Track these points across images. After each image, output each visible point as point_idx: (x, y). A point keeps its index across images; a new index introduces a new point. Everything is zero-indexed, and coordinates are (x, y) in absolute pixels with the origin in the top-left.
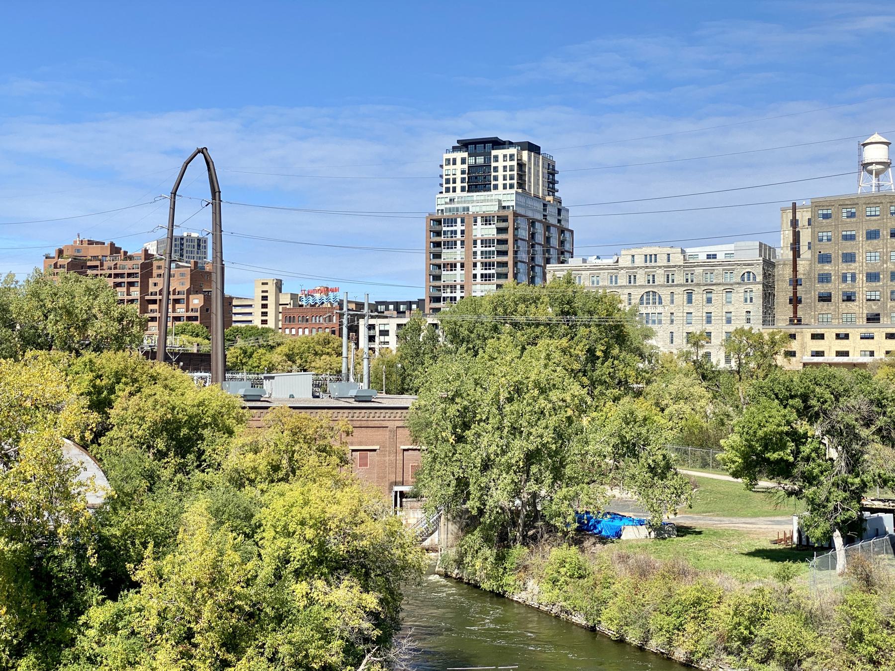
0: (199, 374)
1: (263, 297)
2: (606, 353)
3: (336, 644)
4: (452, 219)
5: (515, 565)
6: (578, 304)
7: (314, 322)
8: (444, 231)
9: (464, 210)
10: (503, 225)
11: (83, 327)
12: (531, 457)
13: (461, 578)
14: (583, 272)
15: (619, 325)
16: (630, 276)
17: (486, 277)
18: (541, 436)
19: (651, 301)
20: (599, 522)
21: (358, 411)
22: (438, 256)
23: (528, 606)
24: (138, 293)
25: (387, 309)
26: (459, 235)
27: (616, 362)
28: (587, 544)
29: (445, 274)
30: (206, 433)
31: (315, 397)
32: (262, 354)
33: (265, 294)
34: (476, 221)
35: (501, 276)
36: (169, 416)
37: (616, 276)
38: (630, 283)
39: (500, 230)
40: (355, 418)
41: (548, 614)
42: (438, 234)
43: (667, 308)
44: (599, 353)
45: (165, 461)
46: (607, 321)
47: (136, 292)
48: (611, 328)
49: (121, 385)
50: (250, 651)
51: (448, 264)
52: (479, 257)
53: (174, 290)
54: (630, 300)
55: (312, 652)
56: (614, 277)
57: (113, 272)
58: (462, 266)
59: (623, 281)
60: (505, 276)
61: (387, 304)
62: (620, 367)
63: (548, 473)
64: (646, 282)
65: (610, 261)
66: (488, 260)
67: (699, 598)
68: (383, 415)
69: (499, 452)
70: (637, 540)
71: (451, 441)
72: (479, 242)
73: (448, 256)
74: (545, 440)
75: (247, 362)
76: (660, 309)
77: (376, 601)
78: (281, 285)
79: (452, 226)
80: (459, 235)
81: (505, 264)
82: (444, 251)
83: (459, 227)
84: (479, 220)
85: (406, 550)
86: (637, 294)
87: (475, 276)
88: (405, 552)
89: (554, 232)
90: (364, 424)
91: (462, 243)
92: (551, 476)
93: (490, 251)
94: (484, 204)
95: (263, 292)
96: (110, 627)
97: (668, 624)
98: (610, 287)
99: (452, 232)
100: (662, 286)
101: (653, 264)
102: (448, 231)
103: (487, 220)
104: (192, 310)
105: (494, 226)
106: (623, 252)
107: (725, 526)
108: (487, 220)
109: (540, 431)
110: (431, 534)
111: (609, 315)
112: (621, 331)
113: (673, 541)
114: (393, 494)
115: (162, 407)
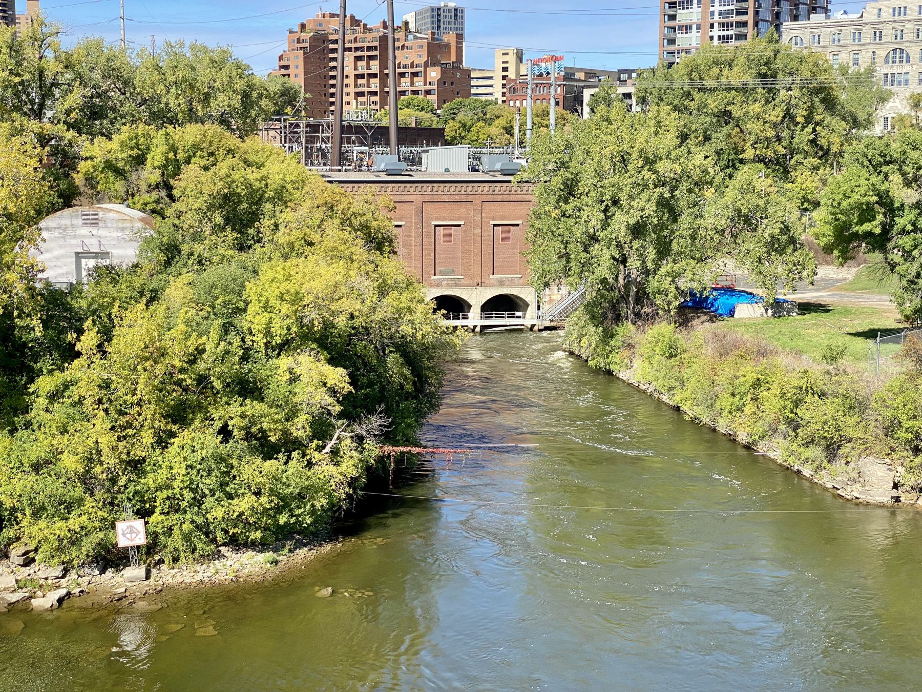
1: (503, 68)
2: (808, 119)
6: (779, 64)
7: (538, 93)
12: (638, 230)
14: (823, 30)
15: (825, 88)
16: (875, 33)
17: (723, 39)
19: (898, 60)
21: (408, 185)
22: (673, 17)
23: (629, 384)
24: (378, 67)
25: (630, 77)
27: (818, 128)
28: (696, 322)
32: (480, 127)
33: (505, 65)
35: (739, 37)
41: (644, 392)
43: (915, 67)
44: (799, 119)
47: (375, 67)
48: (815, 92)
49: (197, 158)
50: (197, 423)
51: (683, 26)
53: (399, 64)
54: (874, 59)
56: (857, 35)
57: (353, 45)
58: (698, 27)
59: (867, 37)
60: (745, 37)
61: (629, 72)
63: (651, 248)
64: (894, 37)
65: (855, 16)
66: (726, 20)
67: (758, 379)
68: (458, 189)
71: (554, 215)
74: (646, 213)
76: (907, 68)
78: (522, 55)
81: (745, 24)
82: (680, 11)
86: (882, 52)
87: (712, 38)
88: (416, 329)
90: (506, 198)
92: (655, 251)
95: (503, 62)
96: (53, 397)
98: (852, 45)
100: (910, 42)
101: (902, 18)
104: (430, 83)
106: (869, 5)
107: (868, 304)
109: (642, 204)
111: (814, 75)
112: (829, 93)
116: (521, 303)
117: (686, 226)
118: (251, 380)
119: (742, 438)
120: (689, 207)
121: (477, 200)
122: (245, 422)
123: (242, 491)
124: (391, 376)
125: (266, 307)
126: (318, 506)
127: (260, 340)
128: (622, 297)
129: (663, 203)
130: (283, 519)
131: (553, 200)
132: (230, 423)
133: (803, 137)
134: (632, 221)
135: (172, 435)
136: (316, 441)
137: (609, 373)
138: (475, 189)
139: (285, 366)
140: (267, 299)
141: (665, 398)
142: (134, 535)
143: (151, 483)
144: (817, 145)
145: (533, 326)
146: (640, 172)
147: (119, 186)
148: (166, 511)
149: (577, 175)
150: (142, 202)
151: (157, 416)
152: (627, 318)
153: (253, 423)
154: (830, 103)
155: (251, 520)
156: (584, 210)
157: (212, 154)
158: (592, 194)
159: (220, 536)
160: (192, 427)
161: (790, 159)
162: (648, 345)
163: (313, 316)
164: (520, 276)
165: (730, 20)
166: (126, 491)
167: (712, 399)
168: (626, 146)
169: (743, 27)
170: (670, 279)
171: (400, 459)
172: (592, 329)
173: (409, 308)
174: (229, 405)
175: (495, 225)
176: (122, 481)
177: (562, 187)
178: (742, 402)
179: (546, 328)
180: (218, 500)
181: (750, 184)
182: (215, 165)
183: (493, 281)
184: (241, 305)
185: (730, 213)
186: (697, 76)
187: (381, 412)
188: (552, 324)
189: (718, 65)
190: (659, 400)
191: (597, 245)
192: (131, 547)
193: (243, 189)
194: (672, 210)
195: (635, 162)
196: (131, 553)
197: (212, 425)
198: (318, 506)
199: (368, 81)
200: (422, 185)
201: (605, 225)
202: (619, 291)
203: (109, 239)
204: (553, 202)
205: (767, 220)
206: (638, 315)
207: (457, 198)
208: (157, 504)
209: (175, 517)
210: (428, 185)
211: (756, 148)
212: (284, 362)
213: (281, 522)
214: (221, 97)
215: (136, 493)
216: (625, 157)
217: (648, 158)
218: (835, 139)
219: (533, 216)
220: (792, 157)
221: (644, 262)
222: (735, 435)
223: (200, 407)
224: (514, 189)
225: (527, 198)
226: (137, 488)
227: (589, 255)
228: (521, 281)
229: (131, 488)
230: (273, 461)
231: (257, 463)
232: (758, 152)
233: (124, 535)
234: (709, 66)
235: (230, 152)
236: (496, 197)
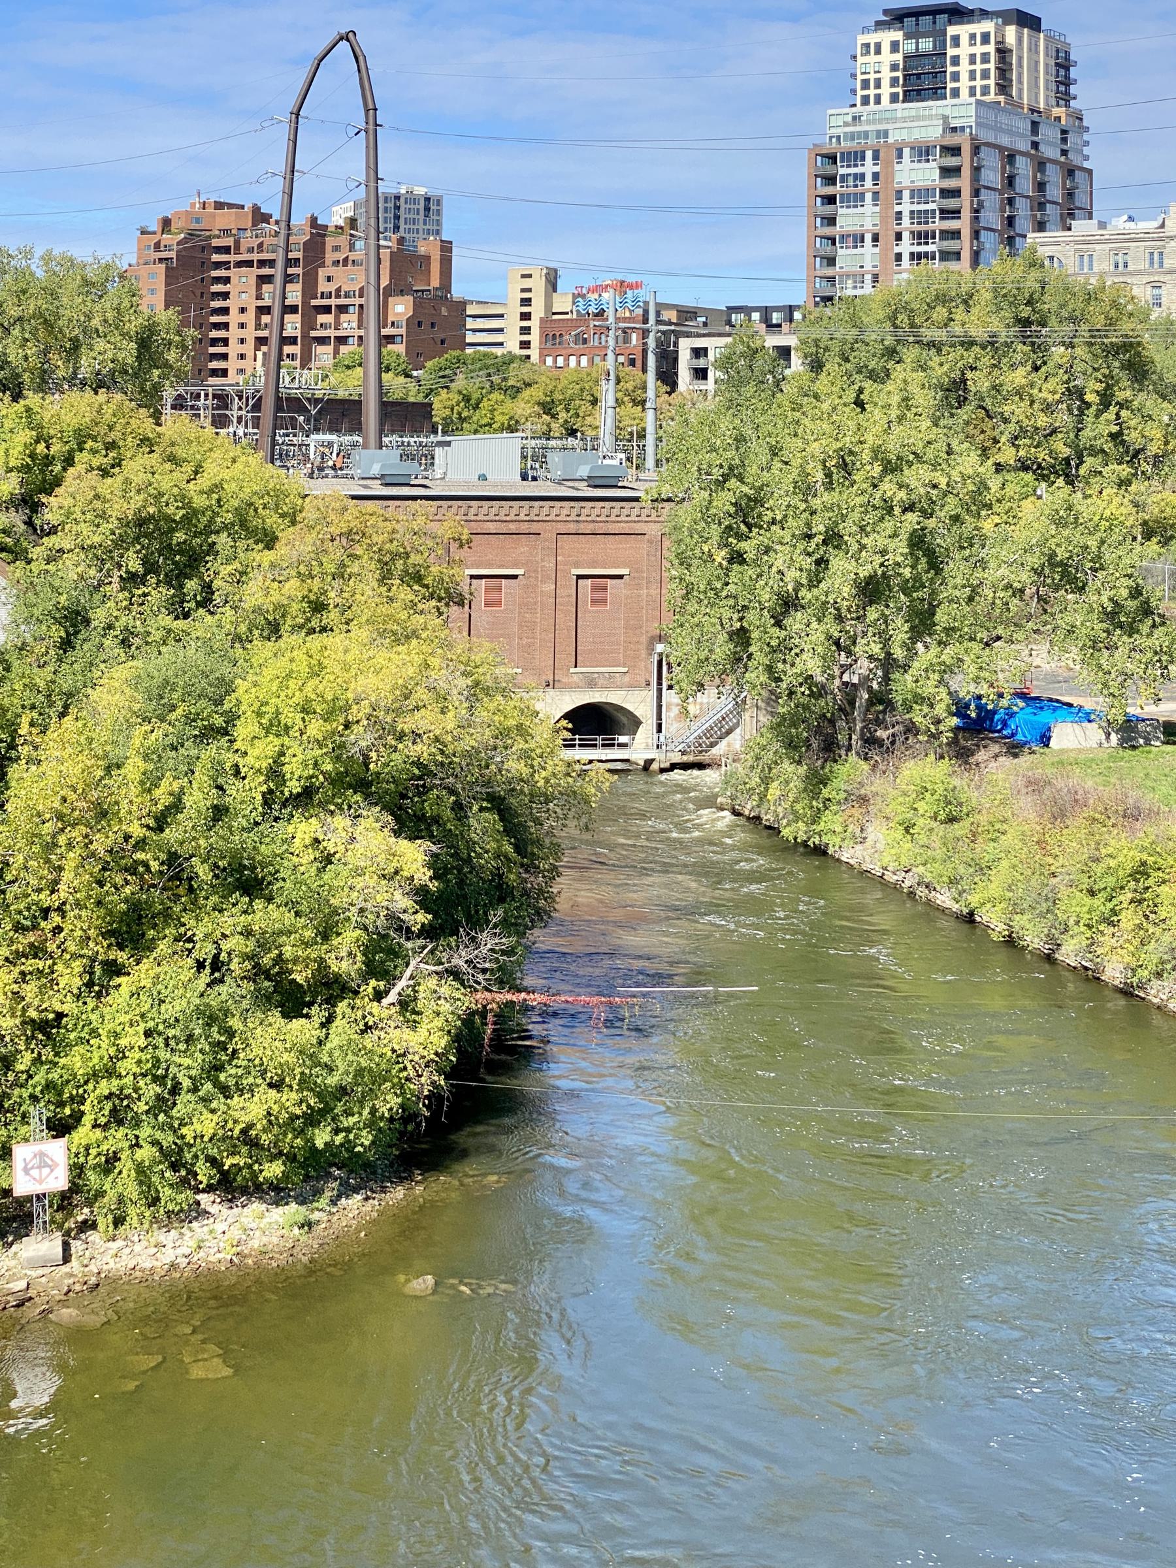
0: (321, 437)
2: (1106, 400)
3: (349, 938)
4: (855, 153)
5: (843, 795)
6: (1049, 304)
8: (842, 176)
10: (951, 161)
11: (74, 350)
13: (758, 818)
14: (1097, 247)
15: (1131, 344)
20: (1012, 715)
22: (831, 221)
28: (981, 756)
31: (524, 477)
34: (900, 156)
35: (946, 256)
36: (151, 510)
37: (1161, 253)
38: (1152, 263)
39: (946, 172)
40: (583, 518)
42: (830, 180)
44: (1090, 397)
45: (140, 592)
46: (1107, 337)
50: (163, 947)
52: (906, 221)
55: (288, 952)
58: (875, 238)
60: (957, 255)
62: (1133, 423)
66: (923, 227)
69: (804, 581)
70: (1080, 751)
72: (906, 194)
73: (848, 219)
77: (421, 858)
79: (856, 166)
81: (956, 234)
82: (841, 211)
83: (869, 167)
84: (906, 152)
87: (899, 257)
89: (1054, 175)
90: (601, 528)
91: (876, 195)
92: (906, 627)
93: (926, 211)
97: (1089, 912)
98: (1149, 274)
99: (855, 176)
103: (923, 152)
110: (728, 733)
111: (1111, 323)
112: (1139, 354)
113: (1149, 752)
114: (656, 658)
115: (139, 492)
116: (624, 720)
117: (959, 581)
118: (246, 862)
120: (962, 548)
122: (251, 944)
123: (251, 1080)
124: (479, 856)
126: (384, 1110)
127: (257, 786)
128: (841, 709)
129: (918, 541)
130: (321, 1137)
131: (715, 531)
132: (226, 946)
133: (1098, 429)
134: (864, 573)
136: (373, 983)
137: (820, 851)
138: (546, 511)
139: (307, 836)
141: (944, 899)
142: (46, 1171)
144: (1123, 442)
146: (875, 486)
148: (103, 1120)
153: (263, 945)
154: (1139, 370)
155: (265, 1139)
156: (775, 551)
159: (204, 1172)
161: (1077, 466)
162: (901, 799)
163: (360, 739)
164: (625, 670)
165: (931, 226)
166: (30, 1082)
167: (1047, 900)
170: (936, 676)
171: (506, 1012)
172: (787, 767)
173: (519, 727)
174: (221, 911)
175: (579, 577)
177: (732, 510)
178: (1110, 905)
179: (673, 767)
180: (206, 1100)
181: (1070, 508)
183: (575, 677)
185: (1034, 560)
186: (906, 320)
187: (495, 927)
188: (685, 759)
189: (944, 302)
190: (929, 903)
191: (799, 614)
192: (38, 1196)
194: (930, 554)
195: (868, 467)
196: (36, 1207)
197: (190, 951)
198: (384, 1110)
199: (337, 319)
200: (450, 503)
201: (815, 581)
204: (715, 539)
205: (1104, 573)
206: (871, 741)
207: (512, 527)
208: (86, 1108)
209: (119, 1135)
210: (460, 503)
211: (1017, 447)
212: (303, 828)
213: (320, 1143)
217: (889, 462)
218: (1154, 432)
219: (676, 562)
220: (1082, 462)
224: (645, 512)
225: (639, 528)
226: (50, 1076)
227: (784, 633)
228: (627, 679)
229: (40, 1078)
230: (303, 1021)
231: (276, 1026)
232: (1022, 453)
233: (26, 1171)
234: (928, 305)
236: (581, 525)
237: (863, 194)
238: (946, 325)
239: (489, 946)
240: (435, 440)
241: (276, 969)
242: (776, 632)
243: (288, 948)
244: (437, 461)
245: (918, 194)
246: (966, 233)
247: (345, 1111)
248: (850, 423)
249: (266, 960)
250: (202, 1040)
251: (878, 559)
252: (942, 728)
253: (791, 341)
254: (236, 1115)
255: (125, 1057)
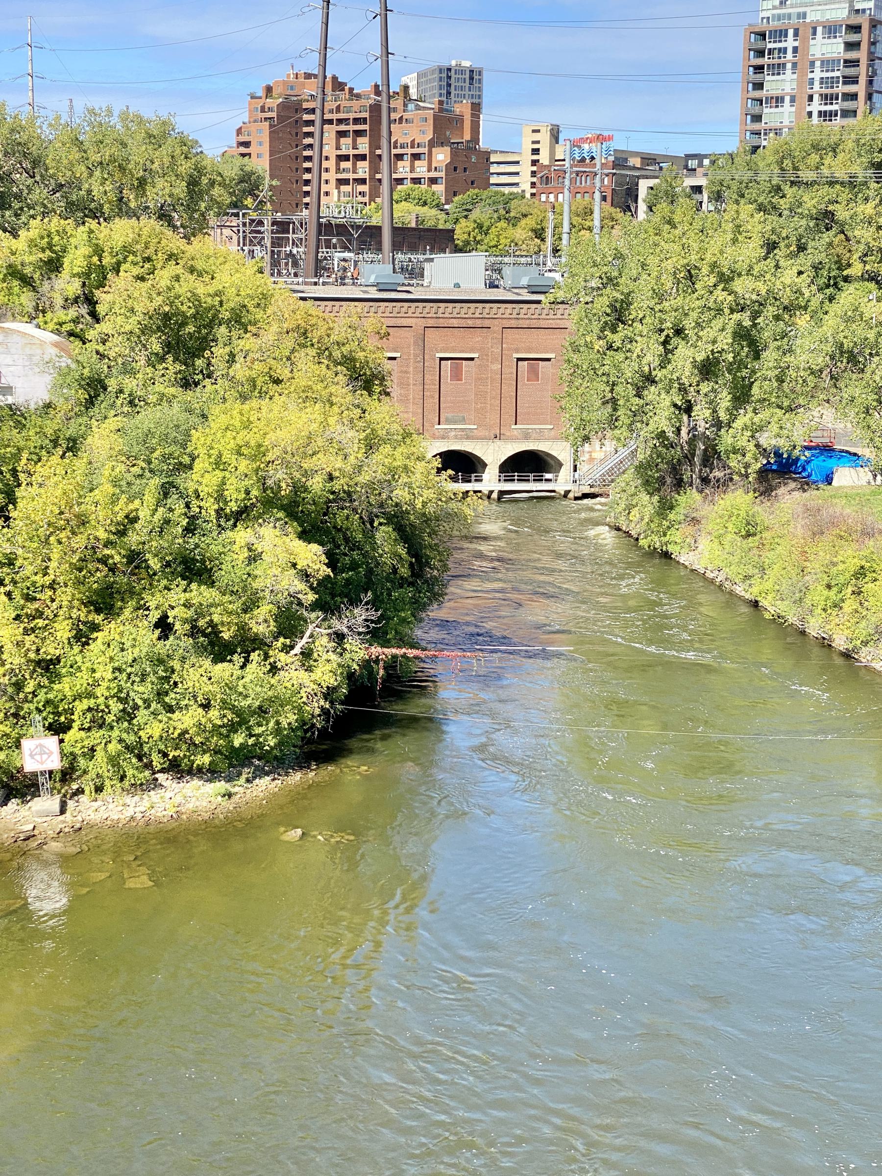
4: (781, 31)
7: (578, 184)
9: (799, 18)
10: (854, 38)
17: (825, 116)
18: (714, 342)
21: (406, 305)
22: (759, 86)
24: (367, 145)
25: (701, 165)
26: (790, 55)
28: (782, 491)
29: (769, 113)
30: (223, 330)
33: (536, 146)
34: (814, 33)
35: (846, 113)
39: (851, 46)
40: (521, 316)
41: (712, 581)
42: (760, 53)
50: (127, 613)
51: (772, 98)
52: (817, 86)
53: (396, 142)
57: (335, 116)
58: (793, 100)
60: (854, 113)
61: (700, 157)
63: (725, 393)
66: (829, 91)
67: (862, 567)
70: (853, 487)
71: (597, 347)
72: (818, 64)
73: (773, 85)
74: (719, 346)
75: (482, 240)
78: (558, 133)
79: (780, 41)
80: (790, 55)
81: (854, 97)
82: (768, 78)
83: (790, 43)
84: (820, 30)
85: (416, 492)
87: (810, 114)
88: (414, 494)
90: (534, 323)
91: (795, 65)
92: (729, 397)
93: (832, 78)
94: (827, 7)
95: (534, 142)
99: (780, 50)
102: (775, 49)
103: (831, 30)
104: (436, 168)
105: (840, 40)
108: (831, 30)
116: (552, 462)
117: (771, 364)
118: (198, 558)
119: (840, 643)
120: (776, 340)
121: (496, 326)
122: (190, 613)
123: (186, 702)
124: (381, 556)
125: (219, 463)
126: (284, 724)
127: (210, 506)
128: (686, 457)
130: (238, 740)
131: (596, 327)
132: (171, 614)
134: (700, 357)
135: (95, 628)
136: (282, 640)
137: (667, 555)
138: (494, 311)
139: (242, 540)
140: (220, 452)
141: (739, 590)
142: (45, 757)
143: (67, 689)
145: (567, 492)
146: (711, 292)
147: (26, 299)
148: (87, 725)
149: (629, 294)
150: (55, 320)
151: (76, 603)
152: (691, 485)
153: (200, 615)
155: (198, 740)
157: (148, 259)
158: (648, 320)
159: (157, 761)
160: (121, 618)
162: (718, 521)
163: (279, 475)
164: (551, 427)
165: (835, 90)
166: (35, 700)
167: (801, 591)
168: (694, 258)
169: (852, 100)
170: (749, 433)
171: (392, 665)
172: (644, 497)
174: (169, 590)
175: (519, 359)
176: (30, 687)
177: (609, 311)
178: (840, 596)
179: (585, 496)
180: (155, 714)
181: (856, 309)
182: (153, 273)
183: (515, 432)
184: (186, 460)
185: (829, 348)
186: (790, 165)
187: (367, 603)
188: (592, 490)
190: (731, 593)
192: (41, 772)
193: (190, 307)
196: (41, 779)
199: (354, 165)
200: (424, 304)
202: (682, 448)
203: (12, 369)
204: (596, 330)
205: (878, 358)
206: (705, 481)
207: (470, 323)
209: (98, 735)
210: (432, 304)
211: (865, 262)
212: (242, 535)
213: (236, 744)
214: (160, 183)
215: (48, 702)
216: (693, 272)
217: (723, 274)
221: (715, 411)
222: (830, 640)
223: (132, 592)
224: (545, 312)
225: (562, 324)
227: (642, 401)
228: (553, 433)
229: (42, 696)
230: (226, 664)
231: (204, 667)
232: (868, 267)
233: (32, 756)
235: (172, 257)
236: (521, 321)
237: (784, 65)
238: (817, 168)
239: (363, 617)
240: (425, 257)
241: (210, 629)
242: (636, 400)
243: (216, 615)
244: (425, 273)
245: (827, 64)
246: (862, 96)
247: (257, 723)
248: (694, 245)
249: (201, 623)
250: (151, 675)
251: (710, 347)
252: (749, 471)
253: (702, 181)
254: (175, 724)
255: (99, 685)
